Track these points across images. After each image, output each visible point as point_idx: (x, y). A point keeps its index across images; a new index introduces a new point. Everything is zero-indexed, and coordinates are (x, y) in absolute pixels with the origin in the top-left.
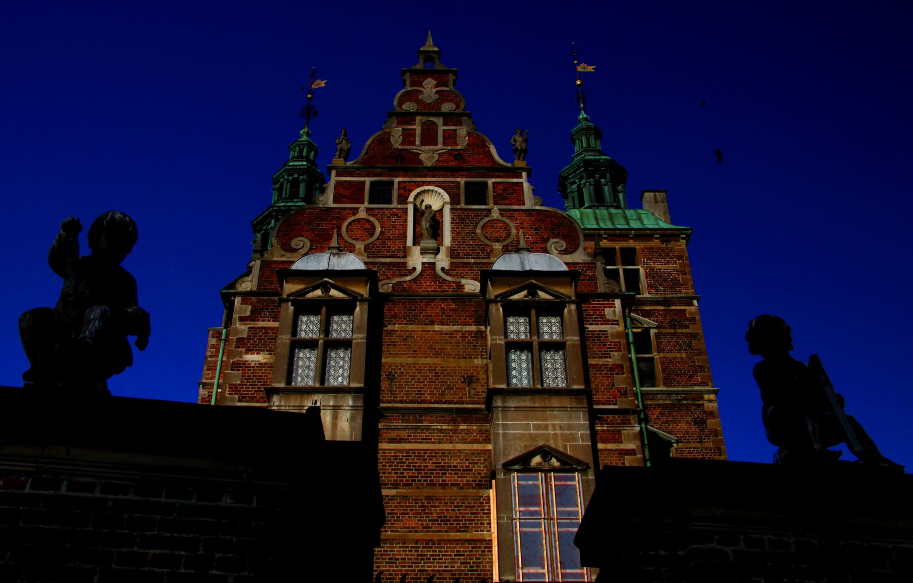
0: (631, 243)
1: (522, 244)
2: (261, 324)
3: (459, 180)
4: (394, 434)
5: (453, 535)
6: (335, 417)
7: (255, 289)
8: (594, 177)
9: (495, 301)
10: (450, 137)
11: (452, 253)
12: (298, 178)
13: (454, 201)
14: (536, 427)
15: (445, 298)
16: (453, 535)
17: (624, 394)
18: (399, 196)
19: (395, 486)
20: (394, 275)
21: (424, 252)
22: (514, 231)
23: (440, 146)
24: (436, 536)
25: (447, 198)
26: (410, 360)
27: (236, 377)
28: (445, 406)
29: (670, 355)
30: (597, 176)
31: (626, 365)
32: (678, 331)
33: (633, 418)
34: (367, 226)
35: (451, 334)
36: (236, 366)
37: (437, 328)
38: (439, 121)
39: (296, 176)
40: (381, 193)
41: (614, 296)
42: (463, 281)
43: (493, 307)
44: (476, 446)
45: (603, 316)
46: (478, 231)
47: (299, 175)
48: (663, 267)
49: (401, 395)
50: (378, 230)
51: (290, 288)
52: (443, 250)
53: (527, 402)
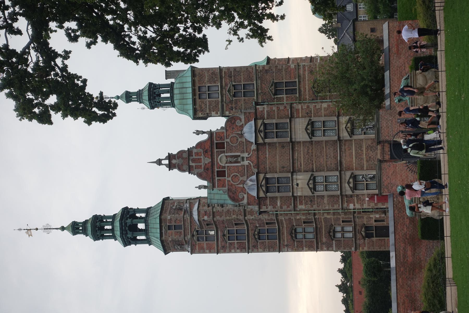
0: (197, 88)
1: (240, 132)
2: (268, 203)
3: (215, 151)
4: (299, 165)
5: (325, 150)
6: (299, 179)
7: (258, 206)
8: (155, 97)
9: (264, 141)
10: (197, 154)
11: (243, 152)
12: (98, 227)
13: (224, 152)
14: (300, 131)
15: (258, 154)
16: (325, 150)
17: (285, 107)
18: (222, 168)
19: (313, 164)
20: (251, 168)
21: (243, 160)
22: (234, 135)
23: (202, 157)
24: (325, 154)
25: (223, 154)
26: (278, 162)
27: (285, 207)
28: (291, 153)
29: (242, 79)
30: (155, 95)
31: (277, 106)
32: (233, 74)
33: (293, 105)
34: (234, 177)
35: (269, 152)
36: (281, 207)
37: (267, 156)
38: (191, 158)
39: (97, 229)
40: (221, 174)
41: (256, 107)
42: (252, 149)
43: (266, 142)
44: (302, 145)
45: (262, 111)
46: (234, 145)
47: (96, 227)
48: (207, 77)
49: (288, 164)
50: (236, 174)
51: (262, 195)
52: (242, 155)
53: (293, 133)
